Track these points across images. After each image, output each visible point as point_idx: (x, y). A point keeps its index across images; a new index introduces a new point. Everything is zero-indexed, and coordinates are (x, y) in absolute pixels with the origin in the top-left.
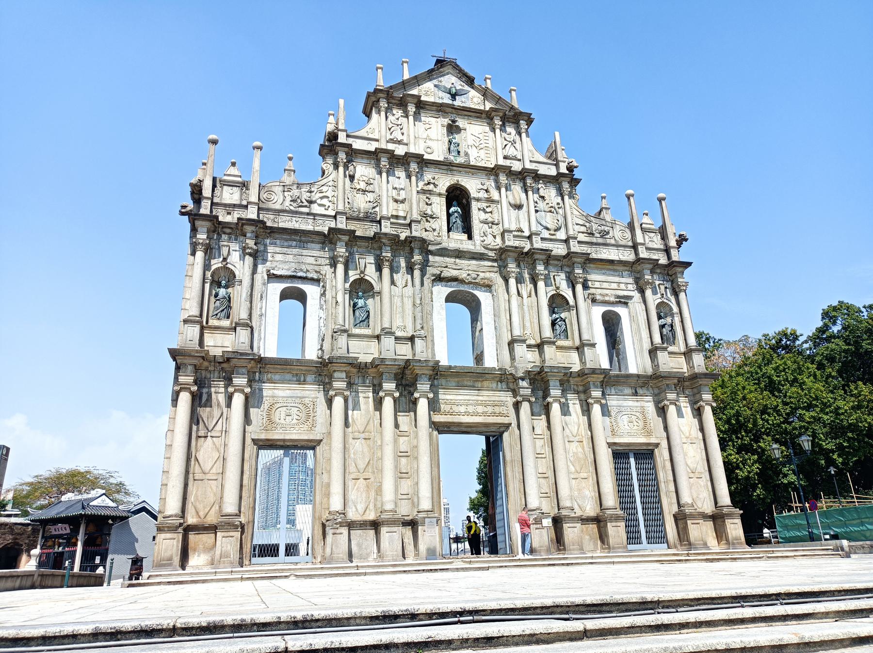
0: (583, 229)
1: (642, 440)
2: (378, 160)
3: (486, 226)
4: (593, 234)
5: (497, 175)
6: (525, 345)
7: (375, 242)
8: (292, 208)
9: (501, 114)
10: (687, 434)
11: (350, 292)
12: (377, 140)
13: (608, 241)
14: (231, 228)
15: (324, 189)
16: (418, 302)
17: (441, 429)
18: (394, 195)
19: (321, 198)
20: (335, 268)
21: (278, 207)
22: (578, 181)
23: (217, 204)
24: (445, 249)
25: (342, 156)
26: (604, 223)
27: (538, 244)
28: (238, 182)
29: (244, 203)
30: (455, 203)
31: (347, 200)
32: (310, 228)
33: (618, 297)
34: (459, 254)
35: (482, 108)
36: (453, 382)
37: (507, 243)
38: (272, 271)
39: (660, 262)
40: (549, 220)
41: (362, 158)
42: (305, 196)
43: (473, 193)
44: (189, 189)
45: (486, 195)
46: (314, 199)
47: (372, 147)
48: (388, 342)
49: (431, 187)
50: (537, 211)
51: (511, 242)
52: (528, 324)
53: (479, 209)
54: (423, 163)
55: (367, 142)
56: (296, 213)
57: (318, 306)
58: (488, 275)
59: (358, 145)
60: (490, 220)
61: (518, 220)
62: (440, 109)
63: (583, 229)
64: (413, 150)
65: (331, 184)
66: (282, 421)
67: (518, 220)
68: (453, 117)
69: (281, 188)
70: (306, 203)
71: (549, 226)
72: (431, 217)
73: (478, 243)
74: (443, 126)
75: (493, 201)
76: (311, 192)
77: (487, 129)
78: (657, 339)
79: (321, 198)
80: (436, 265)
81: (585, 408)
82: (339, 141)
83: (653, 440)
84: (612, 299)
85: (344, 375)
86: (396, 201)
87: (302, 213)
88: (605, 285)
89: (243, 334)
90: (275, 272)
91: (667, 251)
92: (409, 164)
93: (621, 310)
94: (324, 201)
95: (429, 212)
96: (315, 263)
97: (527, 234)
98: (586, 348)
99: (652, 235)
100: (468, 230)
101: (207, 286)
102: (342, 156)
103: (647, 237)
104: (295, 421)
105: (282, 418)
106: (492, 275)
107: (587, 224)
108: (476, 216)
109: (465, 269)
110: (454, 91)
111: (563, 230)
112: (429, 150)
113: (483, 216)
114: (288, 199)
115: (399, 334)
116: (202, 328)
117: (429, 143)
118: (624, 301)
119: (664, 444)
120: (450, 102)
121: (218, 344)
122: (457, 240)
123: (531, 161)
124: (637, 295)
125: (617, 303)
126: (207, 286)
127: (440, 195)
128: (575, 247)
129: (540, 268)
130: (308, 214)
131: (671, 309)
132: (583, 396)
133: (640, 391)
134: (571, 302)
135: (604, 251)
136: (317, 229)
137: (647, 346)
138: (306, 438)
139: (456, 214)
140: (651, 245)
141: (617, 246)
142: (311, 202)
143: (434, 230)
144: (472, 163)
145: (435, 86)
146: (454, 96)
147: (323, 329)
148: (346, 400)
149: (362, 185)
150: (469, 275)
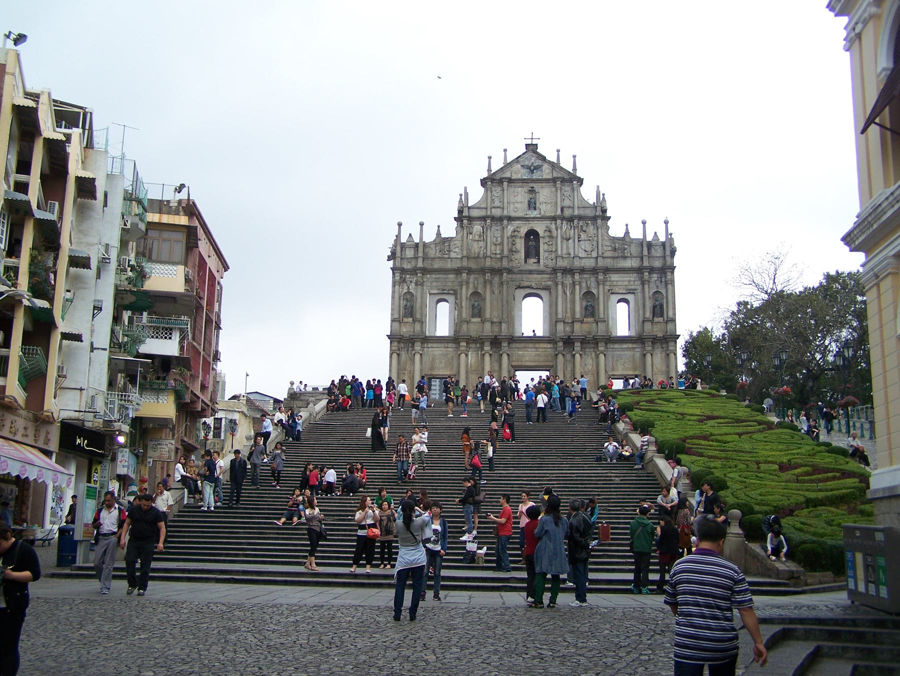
0: (610, 248)
7: (482, 271)
21: (433, 256)
22: (610, 218)
25: (465, 222)
27: (577, 263)
34: (531, 272)
40: (586, 245)
43: (541, 233)
47: (482, 213)
48: (488, 326)
49: (516, 233)
52: (568, 310)
54: (510, 219)
59: (475, 213)
61: (568, 248)
63: (610, 248)
64: (505, 213)
67: (568, 248)
68: (532, 185)
72: (517, 252)
78: (648, 315)
85: (465, 344)
88: (619, 283)
89: (418, 326)
91: (664, 257)
93: (630, 297)
94: (457, 250)
97: (572, 255)
102: (465, 222)
108: (543, 247)
109: (534, 279)
113: (546, 247)
115: (495, 320)
118: (631, 292)
121: (406, 330)
122: (532, 264)
124: (639, 288)
128: (601, 263)
137: (641, 319)
141: (632, 257)
142: (449, 251)
148: (467, 355)
149: (477, 238)
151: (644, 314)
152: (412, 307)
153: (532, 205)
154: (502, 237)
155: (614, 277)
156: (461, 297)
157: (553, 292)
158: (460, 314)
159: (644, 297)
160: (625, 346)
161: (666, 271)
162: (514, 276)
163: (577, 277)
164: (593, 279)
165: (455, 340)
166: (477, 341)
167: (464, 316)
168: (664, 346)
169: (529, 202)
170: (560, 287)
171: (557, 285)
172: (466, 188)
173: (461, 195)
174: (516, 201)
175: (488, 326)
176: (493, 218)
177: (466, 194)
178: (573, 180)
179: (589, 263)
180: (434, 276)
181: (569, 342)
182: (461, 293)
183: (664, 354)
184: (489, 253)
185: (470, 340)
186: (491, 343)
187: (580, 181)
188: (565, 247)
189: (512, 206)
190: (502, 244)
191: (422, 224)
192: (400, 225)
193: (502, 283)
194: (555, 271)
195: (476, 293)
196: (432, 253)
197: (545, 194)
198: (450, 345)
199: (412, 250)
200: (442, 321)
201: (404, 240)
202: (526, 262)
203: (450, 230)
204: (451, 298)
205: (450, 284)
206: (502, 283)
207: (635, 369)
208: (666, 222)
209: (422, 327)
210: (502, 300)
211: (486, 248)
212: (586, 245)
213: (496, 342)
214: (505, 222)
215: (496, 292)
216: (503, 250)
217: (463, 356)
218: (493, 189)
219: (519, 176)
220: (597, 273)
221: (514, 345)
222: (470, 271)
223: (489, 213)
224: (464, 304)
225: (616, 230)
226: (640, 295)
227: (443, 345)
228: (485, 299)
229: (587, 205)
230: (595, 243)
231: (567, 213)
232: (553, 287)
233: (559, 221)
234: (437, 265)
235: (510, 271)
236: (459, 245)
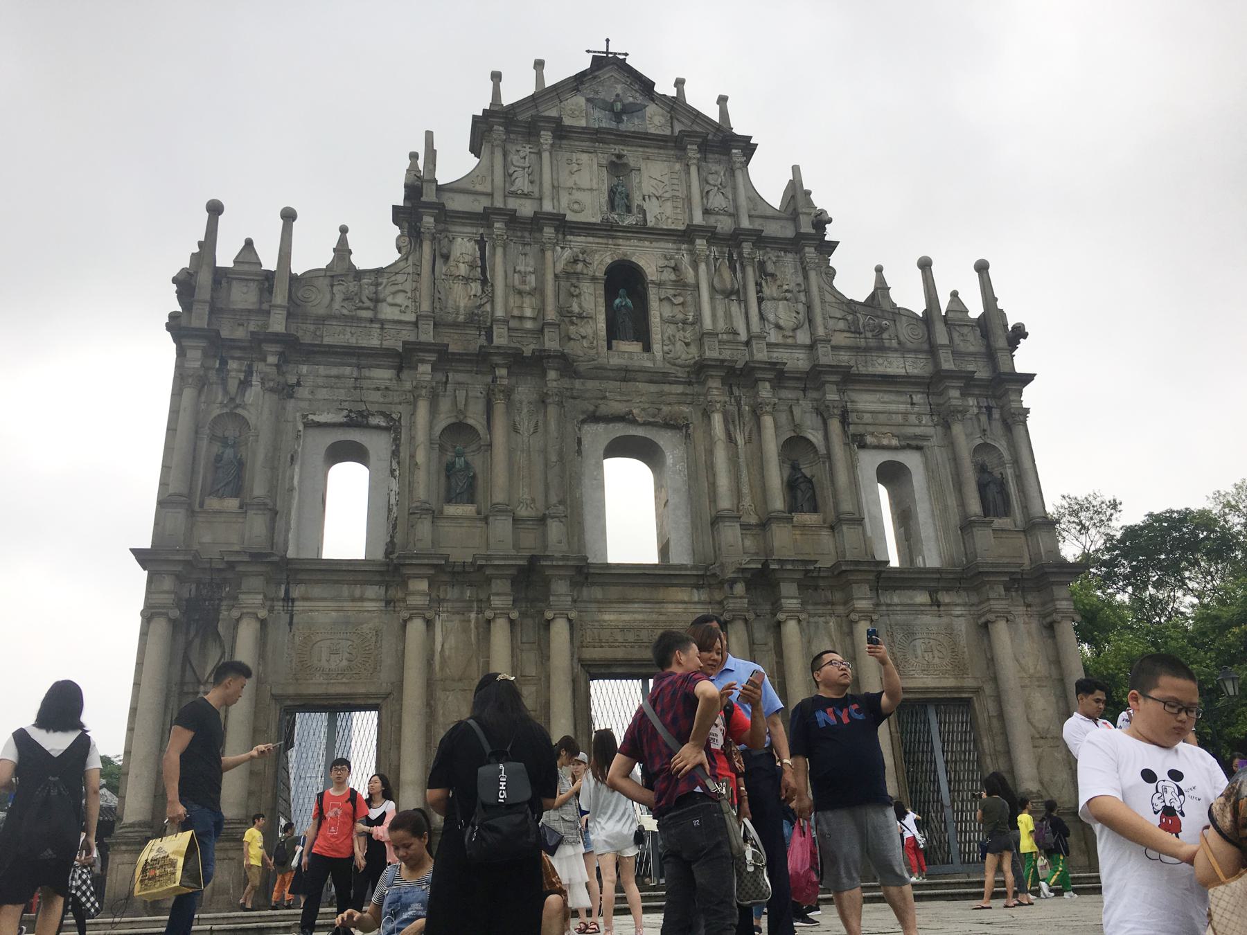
0: (841, 325)
1: (950, 682)
2: (490, 226)
3: (672, 326)
4: (860, 333)
5: (692, 242)
6: (737, 526)
7: (482, 360)
8: (345, 312)
9: (699, 140)
10: (1032, 671)
11: (442, 449)
12: (491, 195)
13: (887, 343)
14: (240, 348)
15: (400, 278)
16: (554, 458)
17: (593, 670)
18: (517, 282)
19: (394, 293)
20: (415, 406)
21: (322, 311)
22: (833, 245)
23: (221, 310)
24: (601, 368)
25: (428, 221)
26: (879, 313)
28: (256, 274)
29: (265, 306)
30: (621, 291)
31: (437, 295)
32: (375, 342)
33: (907, 437)
34: (627, 374)
35: (668, 132)
36: (614, 592)
37: (708, 354)
38: (311, 417)
39: (977, 375)
41: (464, 225)
42: (368, 291)
44: (174, 287)
45: (673, 277)
46: (382, 296)
47: (478, 206)
48: (502, 528)
49: (580, 267)
50: (760, 300)
51: (712, 353)
52: (745, 490)
53: (661, 300)
54: (564, 226)
55: (471, 198)
56: (352, 318)
57: (389, 471)
58: (676, 408)
59: (457, 203)
60: (680, 316)
62: (596, 136)
63: (841, 325)
64: (548, 207)
65: (410, 270)
66: (324, 663)
67: (728, 316)
68: (618, 149)
69: (327, 281)
70: (368, 303)
71: (782, 323)
73: (659, 354)
74: (600, 165)
75: (685, 286)
76: (377, 285)
77: (677, 166)
78: (975, 507)
79: (394, 293)
80: (587, 395)
81: (845, 629)
82: (423, 199)
83: (969, 682)
84: (894, 442)
85: (423, 585)
86: (520, 293)
87: (360, 319)
88: (882, 418)
89: (257, 525)
90: (316, 418)
91: (990, 355)
92: (541, 230)
93: (912, 460)
94: (400, 299)
95: (576, 308)
96: (382, 400)
97: (743, 337)
98: (845, 528)
99: (965, 330)
100: (643, 336)
101: (204, 444)
102: (428, 221)
103: (955, 335)
104: (345, 663)
105: (324, 659)
106: (685, 409)
107: (850, 318)
108: (657, 312)
110: (619, 106)
111: (807, 325)
112: (576, 207)
113: (667, 311)
114: (339, 297)
115: (523, 512)
116: (192, 513)
117: (577, 195)
118: (914, 444)
119: (988, 689)
120: (613, 125)
123: (750, 216)
125: (902, 448)
126: (204, 444)
127: (594, 279)
128: (826, 357)
129: (765, 391)
130: (371, 321)
131: (1000, 456)
132: (840, 609)
133: (945, 598)
134: (822, 450)
135: (880, 361)
136: (386, 344)
137: (955, 520)
138: (362, 690)
139: (624, 311)
140: (962, 347)
141: (902, 349)
142: (377, 301)
143: (583, 337)
144: (650, 224)
145: (588, 100)
146: (618, 117)
147: (395, 509)
148: (429, 624)
149: (463, 270)
150: (643, 409)
151: (962, 504)
152: (241, 464)
153: (618, 198)
154: (539, 273)
155: (867, 402)
156: (412, 439)
157: (698, 435)
158: (408, 487)
159: (955, 460)
160: (922, 598)
161: (1001, 390)
162: (578, 384)
163: (765, 391)
164: (806, 405)
165: (387, 570)
166: (461, 577)
167: (421, 492)
168: (1030, 599)
169: (612, 193)
170: (717, 419)
171: (706, 415)
172: (429, 136)
173: (414, 156)
174: (580, 186)
175: (502, 528)
176: (512, 219)
177: (431, 154)
178: (724, 146)
179: (797, 361)
180: (322, 370)
181: (762, 579)
182: (412, 425)
183: (1034, 625)
184: (499, 313)
185: (447, 573)
186: (515, 582)
187: (747, 147)
188: (720, 313)
189: (565, 200)
190: (539, 291)
191: (289, 216)
192: (215, 209)
193: (543, 401)
194: (700, 370)
195: (459, 429)
196: (319, 302)
197: (654, 179)
198: (372, 591)
199: (253, 285)
200: (347, 514)
201: (225, 257)
202: (609, 347)
203: (377, 248)
204: (378, 444)
205: (376, 396)
206: (543, 401)
207: (959, 668)
208: (982, 268)
209: (272, 529)
210: (544, 451)
211: (492, 300)
212: (783, 314)
213: (530, 578)
214: (549, 232)
215: (525, 425)
216: (541, 310)
217: (416, 628)
218: (512, 148)
219: (583, 123)
220: (820, 387)
221: (585, 593)
222: (444, 359)
223: (499, 204)
224: (421, 457)
225: (853, 283)
226: (939, 455)
227: (345, 590)
228: (490, 445)
229: (769, 213)
230: (801, 307)
231: (724, 225)
232: (696, 419)
233: (700, 243)
234: (335, 336)
235: (567, 365)
236: (408, 286)
